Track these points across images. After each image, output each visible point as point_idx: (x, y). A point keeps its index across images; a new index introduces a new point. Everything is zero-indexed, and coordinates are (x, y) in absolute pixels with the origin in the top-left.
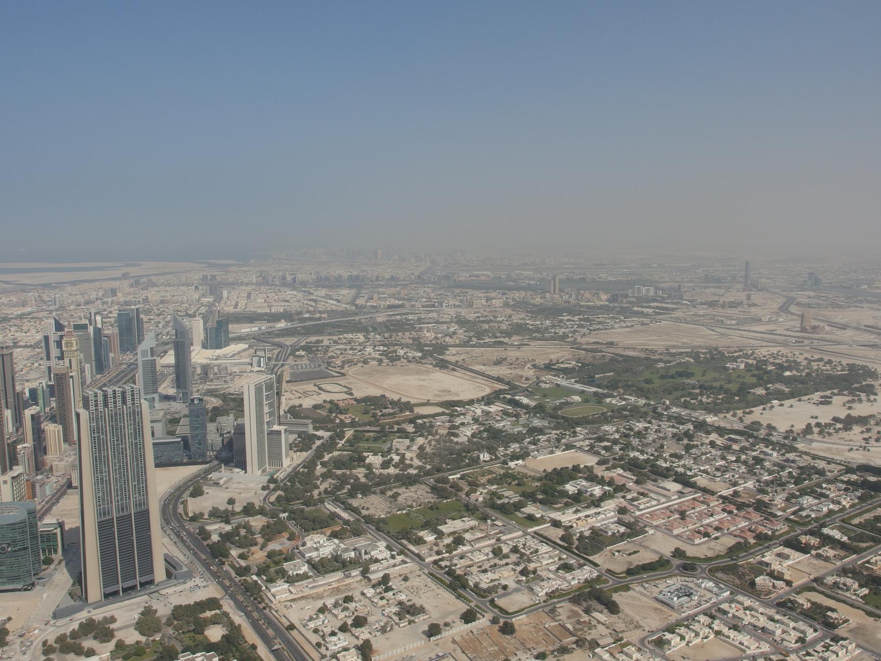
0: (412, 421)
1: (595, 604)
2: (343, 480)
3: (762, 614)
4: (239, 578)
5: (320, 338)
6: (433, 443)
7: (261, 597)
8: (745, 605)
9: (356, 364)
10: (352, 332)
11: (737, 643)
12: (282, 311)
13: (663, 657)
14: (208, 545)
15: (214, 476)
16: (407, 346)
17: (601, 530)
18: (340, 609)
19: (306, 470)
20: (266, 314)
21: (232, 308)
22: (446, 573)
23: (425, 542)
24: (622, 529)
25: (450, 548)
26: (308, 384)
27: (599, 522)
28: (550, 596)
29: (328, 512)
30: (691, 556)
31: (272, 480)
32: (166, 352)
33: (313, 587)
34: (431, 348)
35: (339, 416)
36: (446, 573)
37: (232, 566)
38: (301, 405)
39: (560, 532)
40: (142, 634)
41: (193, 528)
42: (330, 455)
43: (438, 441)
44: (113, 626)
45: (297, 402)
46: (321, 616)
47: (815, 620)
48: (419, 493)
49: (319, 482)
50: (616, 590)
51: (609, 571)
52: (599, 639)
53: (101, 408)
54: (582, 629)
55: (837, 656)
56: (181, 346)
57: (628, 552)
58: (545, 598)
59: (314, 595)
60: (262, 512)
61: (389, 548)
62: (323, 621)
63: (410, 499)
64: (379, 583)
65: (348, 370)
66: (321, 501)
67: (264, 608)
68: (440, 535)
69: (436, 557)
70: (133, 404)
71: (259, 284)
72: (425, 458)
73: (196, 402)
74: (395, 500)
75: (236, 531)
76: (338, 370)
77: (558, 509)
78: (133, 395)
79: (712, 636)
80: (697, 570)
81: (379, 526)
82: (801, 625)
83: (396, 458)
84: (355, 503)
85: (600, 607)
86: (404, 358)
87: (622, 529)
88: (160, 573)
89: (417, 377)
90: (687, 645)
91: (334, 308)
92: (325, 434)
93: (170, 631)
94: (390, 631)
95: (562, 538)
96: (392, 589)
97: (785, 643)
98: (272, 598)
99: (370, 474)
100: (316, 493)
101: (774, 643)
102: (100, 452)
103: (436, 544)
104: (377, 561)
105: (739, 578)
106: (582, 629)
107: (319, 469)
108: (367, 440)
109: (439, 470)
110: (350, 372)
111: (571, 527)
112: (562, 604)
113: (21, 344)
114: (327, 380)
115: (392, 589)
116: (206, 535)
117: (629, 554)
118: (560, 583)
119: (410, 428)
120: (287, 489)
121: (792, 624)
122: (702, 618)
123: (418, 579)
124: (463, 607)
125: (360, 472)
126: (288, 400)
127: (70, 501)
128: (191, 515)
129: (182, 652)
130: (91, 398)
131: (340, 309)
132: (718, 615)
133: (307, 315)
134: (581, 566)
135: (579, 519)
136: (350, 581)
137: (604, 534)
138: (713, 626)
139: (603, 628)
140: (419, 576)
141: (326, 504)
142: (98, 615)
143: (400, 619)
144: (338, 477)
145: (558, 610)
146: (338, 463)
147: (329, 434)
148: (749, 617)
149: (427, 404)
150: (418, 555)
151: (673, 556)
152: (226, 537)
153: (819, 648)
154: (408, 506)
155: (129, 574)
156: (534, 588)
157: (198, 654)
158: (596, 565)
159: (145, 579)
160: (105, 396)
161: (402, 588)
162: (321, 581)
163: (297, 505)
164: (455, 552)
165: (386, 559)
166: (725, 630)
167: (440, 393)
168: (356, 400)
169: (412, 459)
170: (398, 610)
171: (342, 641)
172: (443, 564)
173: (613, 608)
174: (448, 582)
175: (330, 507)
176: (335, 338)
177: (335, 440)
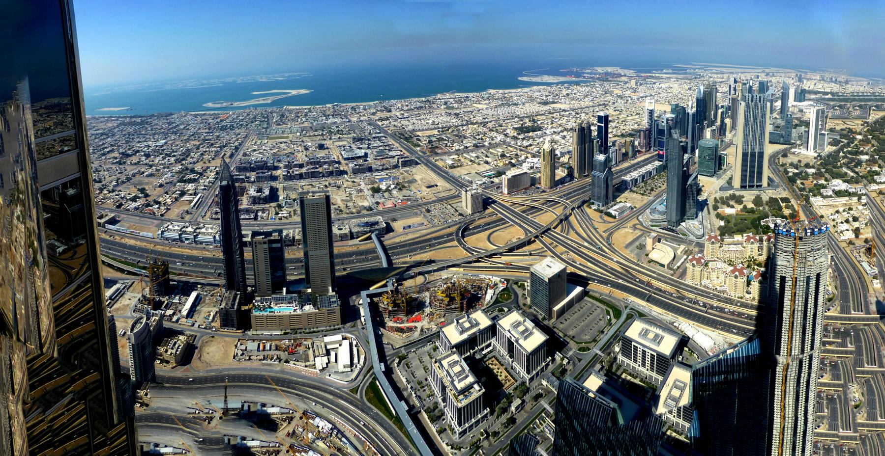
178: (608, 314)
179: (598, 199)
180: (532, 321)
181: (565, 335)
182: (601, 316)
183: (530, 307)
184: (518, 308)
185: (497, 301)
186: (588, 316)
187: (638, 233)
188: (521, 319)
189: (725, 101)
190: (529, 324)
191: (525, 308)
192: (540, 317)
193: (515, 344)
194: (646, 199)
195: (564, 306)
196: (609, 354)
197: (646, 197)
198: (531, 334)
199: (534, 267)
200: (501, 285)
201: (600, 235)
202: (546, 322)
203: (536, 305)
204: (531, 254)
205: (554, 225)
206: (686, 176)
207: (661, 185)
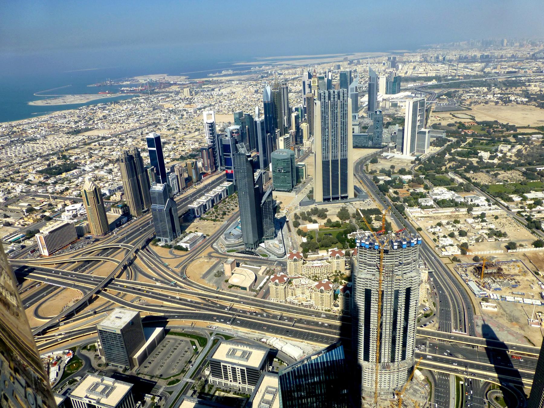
0: (515, 136)
2: (462, 163)
4: (392, 203)
5: (457, 90)
6: (528, 149)
7: (404, 213)
9: (480, 104)
10: (479, 87)
12: (434, 75)
14: (377, 185)
15: (384, 154)
16: (517, 95)
18: (450, 226)
19: (439, 156)
20: (424, 77)
21: (403, 74)
22: (526, 219)
23: (513, 201)
25: (530, 207)
26: (446, 113)
29: (450, 178)
31: (418, 159)
32: (364, 96)
33: (435, 213)
34: (536, 97)
35: (464, 130)
36: (526, 219)
37: (390, 197)
38: (440, 124)
40: (341, 219)
41: (370, 177)
42: (455, 150)
43: (532, 148)
44: (327, 213)
45: (438, 122)
46: (438, 227)
48: (513, 175)
49: (446, 163)
53: (327, 100)
56: (372, 90)
59: (435, 217)
60: (409, 173)
61: (488, 200)
62: (439, 230)
63: (506, 177)
64: (478, 217)
65: (474, 107)
66: (446, 172)
67: (405, 218)
68: (525, 199)
69: (520, 210)
70: (343, 99)
71: (421, 62)
72: (521, 157)
73: (378, 113)
74: (496, 177)
75: (394, 181)
76: (467, 106)
78: (344, 94)
81: (484, 189)
83: (500, 155)
84: (468, 175)
86: (515, 102)
88: (351, 193)
89: (523, 112)
91: (468, 73)
92: (454, 140)
93: (354, 221)
94: (481, 242)
96: (486, 221)
98: (410, 214)
99: (480, 161)
100: (444, 168)
102: (325, 125)
103: (521, 203)
104: (478, 206)
107: (447, 156)
108: (482, 144)
109: (530, 164)
110: (475, 108)
113: (293, 91)
114: (459, 112)
115: (486, 221)
116: (377, 181)
119: (512, 140)
120: (426, 164)
123: (505, 220)
124: (536, 238)
125: (474, 160)
126: (433, 119)
127: (310, 160)
128: (369, 171)
129: (360, 229)
130: (322, 94)
131: (473, 74)
133: (450, 78)
136: (458, 213)
140: (506, 218)
141: (449, 174)
142: (320, 207)
143: (489, 237)
144: (459, 161)
146: (460, 154)
147: (456, 139)
149: (528, 127)
150: (507, 207)
152: (387, 183)
154: (505, 181)
155: (335, 191)
157: (367, 232)
159: (343, 195)
160: (329, 93)
161: (492, 222)
162: (441, 210)
163: (431, 172)
164: (534, 209)
165: (484, 205)
167: (538, 122)
168: (477, 123)
169: (511, 156)
170: (488, 232)
171: (449, 241)
172: (524, 214)
174: (526, 224)
175: (451, 175)
176: (468, 90)
177: (460, 142)
178: (193, 344)
179: (164, 234)
180: (112, 377)
181: (152, 377)
182: (186, 349)
183: (107, 365)
184: (92, 370)
185: (65, 375)
186: (173, 352)
187: (214, 261)
188: (99, 380)
189: (300, 103)
190: (109, 381)
191: (100, 368)
192: (121, 370)
193: (97, 405)
194: (219, 225)
195: (145, 351)
196: (200, 378)
197: (219, 223)
198: (113, 388)
199: (101, 324)
200: (66, 357)
201: (173, 271)
202: (128, 373)
203: (113, 360)
204: (95, 313)
205: (117, 274)
206: (259, 194)
207: (234, 208)
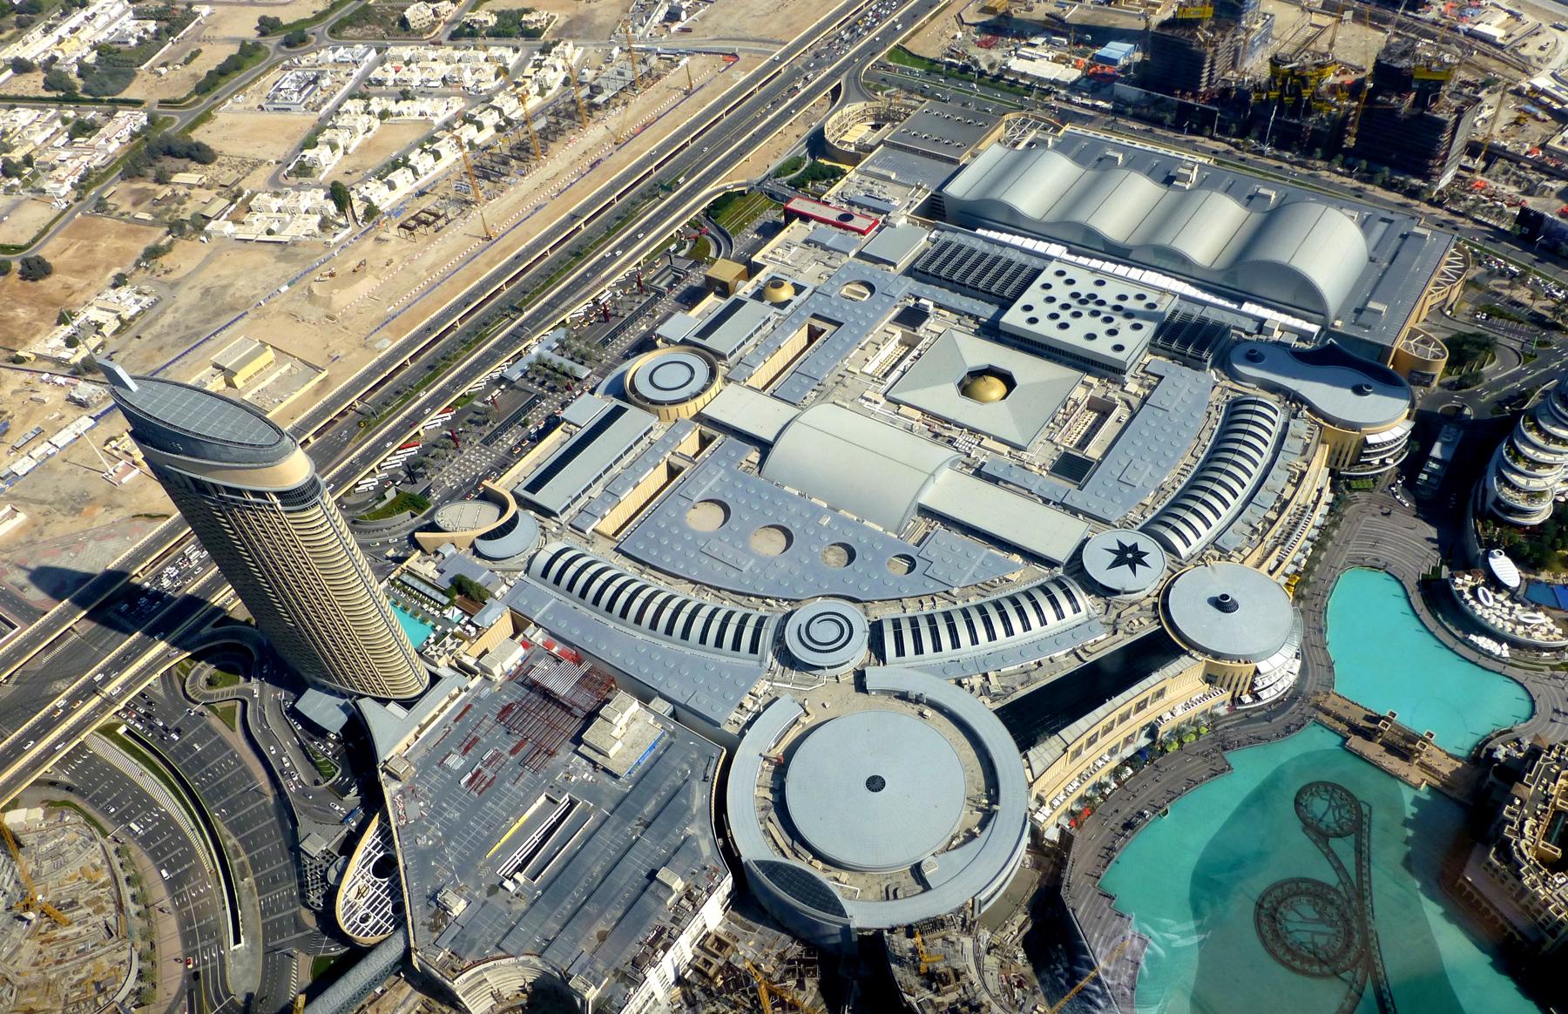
1: (168, 162)
3: (434, 60)
8: (406, 58)
11: (416, 117)
13: (319, 186)
17: (112, 43)
24: (152, 26)
27: (103, 29)
28: (83, 187)
30: (291, 21)
39: (38, 78)
47: (509, 35)
50: (193, 127)
51: (164, 103)
52: (204, 209)
54: (168, 210)
55: (555, 70)
57: (182, 60)
58: (75, 194)
77: (11, 40)
79: (376, 123)
80: (310, 40)
82: (494, 51)
85: (180, 163)
87: (152, 26)
90: (345, 153)
95: (48, 86)
97: (483, 87)
101: (466, 94)
105: (381, 24)
106: (168, 210)
111: (54, 59)
112: (113, 189)
117: (187, 62)
118: (88, 158)
121: (482, 55)
122: (349, 105)
132: (373, 89)
134: (110, 116)
135: (61, 40)
137: (122, 47)
138: (371, 108)
139: (203, 191)
145: (108, 201)
148: (418, 72)
151: (263, 34)
153: (529, 71)
156: (45, 187)
158: (136, 103)
166: (393, 107)
173: (201, 155)
